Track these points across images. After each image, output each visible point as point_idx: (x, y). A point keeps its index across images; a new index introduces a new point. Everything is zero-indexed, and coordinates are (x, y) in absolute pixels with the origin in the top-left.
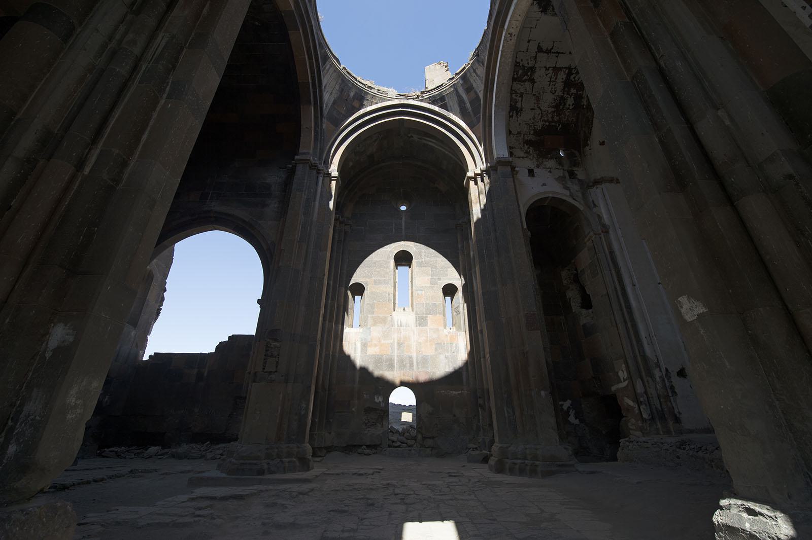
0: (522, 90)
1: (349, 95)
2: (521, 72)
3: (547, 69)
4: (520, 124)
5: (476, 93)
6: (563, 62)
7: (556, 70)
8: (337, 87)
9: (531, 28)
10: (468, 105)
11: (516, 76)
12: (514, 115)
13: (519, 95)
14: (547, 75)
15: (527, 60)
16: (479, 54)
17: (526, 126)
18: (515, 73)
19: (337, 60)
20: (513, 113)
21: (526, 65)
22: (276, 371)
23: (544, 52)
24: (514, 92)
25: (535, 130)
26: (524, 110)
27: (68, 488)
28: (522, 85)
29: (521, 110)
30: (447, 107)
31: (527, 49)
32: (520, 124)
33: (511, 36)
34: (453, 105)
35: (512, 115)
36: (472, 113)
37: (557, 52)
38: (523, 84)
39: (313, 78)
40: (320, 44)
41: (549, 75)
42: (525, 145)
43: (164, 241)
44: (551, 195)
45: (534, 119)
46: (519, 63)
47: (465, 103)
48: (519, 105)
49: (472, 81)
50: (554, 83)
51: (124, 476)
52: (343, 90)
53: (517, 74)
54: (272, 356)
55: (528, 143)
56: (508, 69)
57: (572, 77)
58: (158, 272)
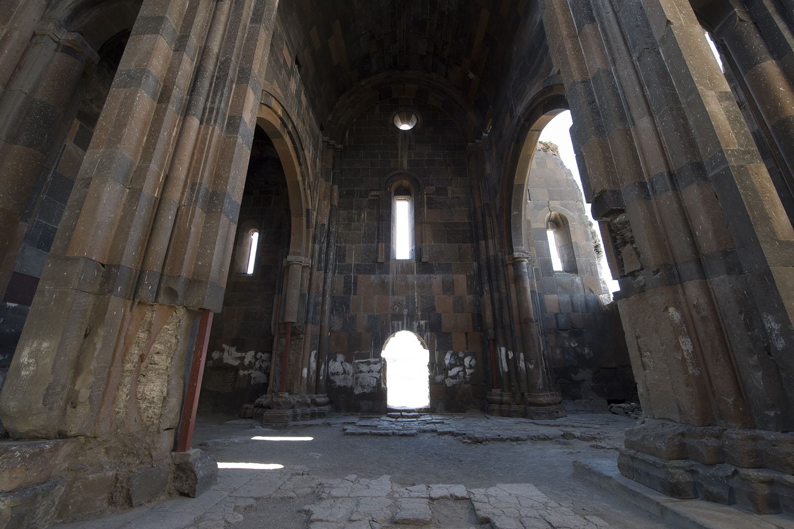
22: (642, 269)
27: (481, 443)
43: (513, 182)
51: (551, 439)
54: (625, 243)
58: (569, 212)
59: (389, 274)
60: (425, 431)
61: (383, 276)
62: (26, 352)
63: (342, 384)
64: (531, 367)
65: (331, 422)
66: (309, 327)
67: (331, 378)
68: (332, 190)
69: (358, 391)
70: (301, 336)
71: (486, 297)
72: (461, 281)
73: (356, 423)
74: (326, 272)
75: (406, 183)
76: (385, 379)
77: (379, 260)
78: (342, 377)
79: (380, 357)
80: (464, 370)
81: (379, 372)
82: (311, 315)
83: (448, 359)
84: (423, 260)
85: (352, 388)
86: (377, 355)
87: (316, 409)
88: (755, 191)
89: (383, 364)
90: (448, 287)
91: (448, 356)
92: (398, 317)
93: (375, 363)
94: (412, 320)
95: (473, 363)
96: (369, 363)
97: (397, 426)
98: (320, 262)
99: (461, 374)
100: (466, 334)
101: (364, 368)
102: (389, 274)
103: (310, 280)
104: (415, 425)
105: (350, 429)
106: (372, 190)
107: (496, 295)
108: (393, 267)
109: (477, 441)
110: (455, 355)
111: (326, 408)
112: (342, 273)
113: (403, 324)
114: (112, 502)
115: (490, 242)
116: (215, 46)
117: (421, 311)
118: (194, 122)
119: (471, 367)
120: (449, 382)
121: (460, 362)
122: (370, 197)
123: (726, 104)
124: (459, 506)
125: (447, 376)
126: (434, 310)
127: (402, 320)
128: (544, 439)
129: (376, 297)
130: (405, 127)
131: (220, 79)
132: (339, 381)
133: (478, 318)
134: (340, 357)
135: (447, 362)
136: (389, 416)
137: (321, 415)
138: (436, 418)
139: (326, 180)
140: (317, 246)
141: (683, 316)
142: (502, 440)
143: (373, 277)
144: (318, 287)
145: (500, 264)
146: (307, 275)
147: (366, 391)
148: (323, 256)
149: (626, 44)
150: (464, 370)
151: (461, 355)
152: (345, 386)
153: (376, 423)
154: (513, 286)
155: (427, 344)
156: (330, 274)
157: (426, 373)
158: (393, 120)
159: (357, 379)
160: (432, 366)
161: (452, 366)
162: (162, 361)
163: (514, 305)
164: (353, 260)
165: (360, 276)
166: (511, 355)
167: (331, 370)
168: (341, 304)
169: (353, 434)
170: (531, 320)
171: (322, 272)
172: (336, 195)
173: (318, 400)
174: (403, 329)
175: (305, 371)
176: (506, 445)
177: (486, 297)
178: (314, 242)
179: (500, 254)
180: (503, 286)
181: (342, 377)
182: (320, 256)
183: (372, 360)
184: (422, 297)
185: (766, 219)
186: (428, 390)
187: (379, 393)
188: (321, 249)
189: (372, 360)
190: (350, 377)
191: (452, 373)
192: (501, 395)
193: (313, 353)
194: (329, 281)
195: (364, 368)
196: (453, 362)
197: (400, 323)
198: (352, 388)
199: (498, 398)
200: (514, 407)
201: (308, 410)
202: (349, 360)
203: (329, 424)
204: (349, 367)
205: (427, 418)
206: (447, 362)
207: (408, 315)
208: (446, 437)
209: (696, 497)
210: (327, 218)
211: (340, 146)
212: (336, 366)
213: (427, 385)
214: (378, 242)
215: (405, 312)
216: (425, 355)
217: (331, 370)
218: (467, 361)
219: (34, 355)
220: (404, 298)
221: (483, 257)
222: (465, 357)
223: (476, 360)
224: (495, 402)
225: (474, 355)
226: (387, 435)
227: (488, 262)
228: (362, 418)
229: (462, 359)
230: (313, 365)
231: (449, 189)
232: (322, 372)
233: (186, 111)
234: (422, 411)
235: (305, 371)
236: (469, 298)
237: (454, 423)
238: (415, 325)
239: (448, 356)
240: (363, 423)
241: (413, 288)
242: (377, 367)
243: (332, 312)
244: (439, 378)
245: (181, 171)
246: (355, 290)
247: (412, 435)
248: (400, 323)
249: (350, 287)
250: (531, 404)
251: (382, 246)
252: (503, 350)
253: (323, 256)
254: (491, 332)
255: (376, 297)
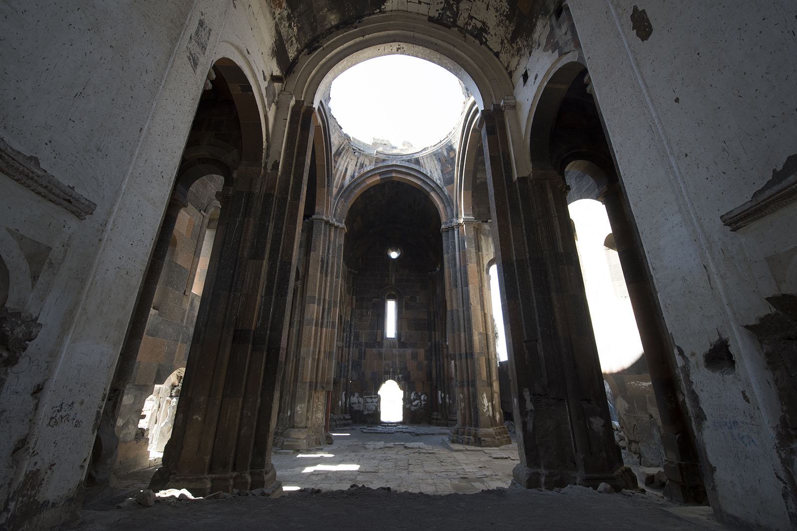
0: (466, 15)
1: (445, 156)
2: (448, 13)
4: (496, 35)
8: (436, 162)
9: (407, 2)
11: (452, 20)
12: (486, 36)
13: (470, 21)
15: (438, 4)
17: (500, 28)
18: (449, 19)
19: (424, 149)
20: (484, 37)
21: (443, 5)
24: (466, 26)
25: (507, 17)
26: (485, 21)
28: (461, 14)
29: (484, 23)
31: (428, 4)
32: (496, 35)
33: (400, 49)
35: (486, 39)
38: (460, 12)
39: (320, 286)
40: (409, 161)
42: (513, 45)
44: (545, 84)
45: (497, 11)
46: (439, 14)
48: (479, 25)
52: (439, 159)
53: (450, 17)
55: (512, 40)
56: (428, 51)
59: (382, 348)
60: (398, 432)
61: (380, 349)
62: (298, 407)
63: (358, 409)
64: (451, 402)
65: (355, 428)
66: (342, 379)
67: (352, 405)
68: (352, 299)
69: (366, 413)
70: (338, 384)
71: (433, 363)
72: (422, 352)
73: (366, 428)
74: (349, 348)
75: (393, 293)
76: (380, 406)
77: (378, 340)
78: (357, 405)
79: (377, 395)
80: (421, 402)
81: (377, 403)
82: (343, 373)
83: (413, 396)
84: (402, 341)
85: (363, 411)
86: (376, 393)
87: (345, 422)
88: (480, 366)
89: (379, 398)
90: (415, 356)
91: (413, 394)
92: (387, 373)
93: (375, 398)
94: (395, 374)
95: (426, 398)
96: (371, 398)
97: (386, 430)
98: (346, 343)
99: (419, 404)
100: (423, 382)
101: (369, 400)
102: (382, 348)
103: (342, 354)
104: (394, 429)
105: (365, 431)
106: (374, 297)
107: (438, 363)
108: (385, 343)
109: (417, 435)
110: (416, 394)
111: (350, 421)
112: (357, 347)
113: (390, 377)
114: (316, 444)
115: (437, 332)
116: (327, 297)
117: (400, 370)
118: (324, 329)
119: (424, 400)
120: (413, 408)
121: (419, 397)
122: (373, 302)
123: (480, 336)
124: (401, 446)
125: (412, 405)
126: (406, 368)
127: (390, 374)
128: (443, 434)
129: (376, 361)
130: (394, 255)
131: (329, 309)
132: (356, 407)
133: (429, 374)
134: (357, 395)
135: (412, 397)
136: (382, 426)
137: (348, 425)
138: (405, 427)
139: (350, 294)
140: (345, 334)
141: (464, 396)
142: (428, 434)
143: (374, 350)
144: (345, 358)
145: (440, 346)
146: (340, 351)
147: (370, 412)
148: (348, 339)
149: (463, 302)
150: (421, 402)
151: (420, 394)
152: (359, 410)
153: (375, 429)
154: (445, 359)
155: (401, 388)
156: (351, 349)
157: (401, 403)
158: (388, 249)
159: (365, 406)
160: (404, 399)
161: (415, 400)
162: (321, 407)
163: (446, 369)
164: (363, 339)
165: (367, 349)
166: (443, 395)
167: (352, 401)
168: (357, 365)
169: (366, 432)
170: (453, 379)
171: (347, 349)
172: (354, 302)
173: (346, 417)
174: (390, 379)
175: (340, 402)
176: (428, 436)
177: (433, 363)
178: (344, 332)
179: (441, 341)
180: (441, 359)
181: (357, 405)
182: (346, 340)
183: (373, 396)
184: (401, 362)
185: (480, 373)
186: (402, 413)
187: (377, 414)
188: (347, 335)
189: (373, 396)
190: (361, 405)
191: (414, 403)
192: (437, 416)
193: (344, 393)
194: (351, 353)
195: (369, 400)
196: (415, 398)
197: (388, 376)
198: (363, 411)
199: (436, 417)
200: (442, 421)
201: (342, 422)
202: (361, 396)
203: (353, 429)
204: (361, 400)
205: (401, 426)
206: (412, 397)
207: (392, 372)
208: (406, 434)
209: (457, 443)
210: (350, 317)
211: (357, 272)
212: (354, 399)
213: (402, 410)
214: (377, 330)
215: (391, 370)
216: (401, 393)
217: (352, 401)
218: (422, 397)
219: (300, 408)
220: (391, 363)
221: (433, 341)
222: (421, 395)
223: (427, 396)
224: (433, 419)
225: (426, 395)
226: (381, 433)
227: (435, 344)
228: (368, 427)
229: (420, 396)
230: (344, 399)
231: (417, 297)
232: (348, 402)
233: (322, 327)
234: (398, 423)
235: (340, 402)
236: (426, 362)
237: (412, 429)
238: (396, 377)
239: (413, 394)
240: (370, 428)
241: (396, 356)
242: (376, 400)
243: (352, 370)
244: (408, 406)
245: (323, 350)
246: (364, 357)
247: (392, 433)
248: (388, 376)
249: (362, 355)
250: (450, 420)
251: (379, 331)
252: (440, 392)
253: (348, 339)
254: (435, 382)
255: (376, 361)
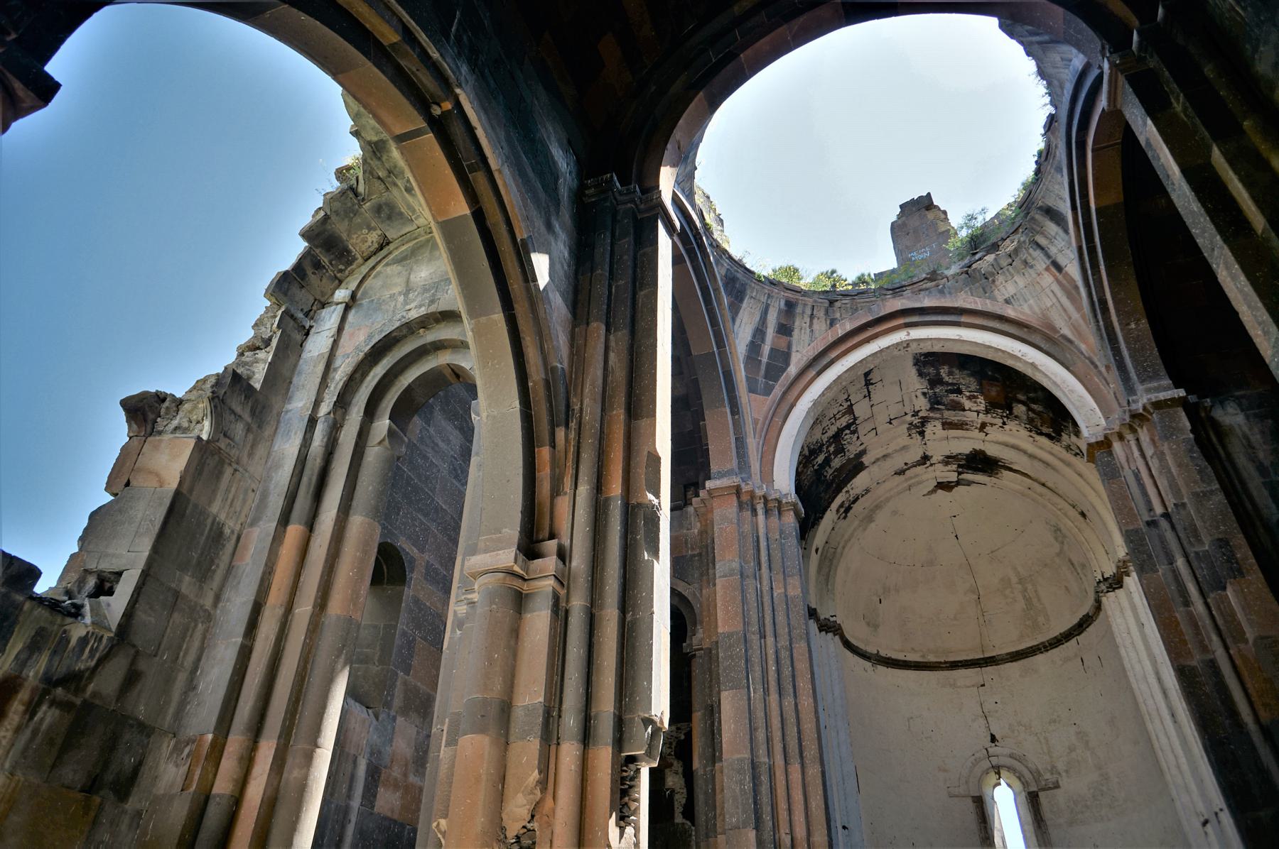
3: (847, 400)
5: (789, 346)
6: (861, 410)
7: (850, 410)
10: (766, 349)
14: (841, 405)
16: (838, 304)
23: (866, 380)
30: (737, 315)
33: (904, 348)
34: (746, 324)
36: (763, 367)
37: (869, 392)
41: (841, 408)
47: (763, 340)
49: (797, 323)
50: (834, 421)
57: (847, 432)
